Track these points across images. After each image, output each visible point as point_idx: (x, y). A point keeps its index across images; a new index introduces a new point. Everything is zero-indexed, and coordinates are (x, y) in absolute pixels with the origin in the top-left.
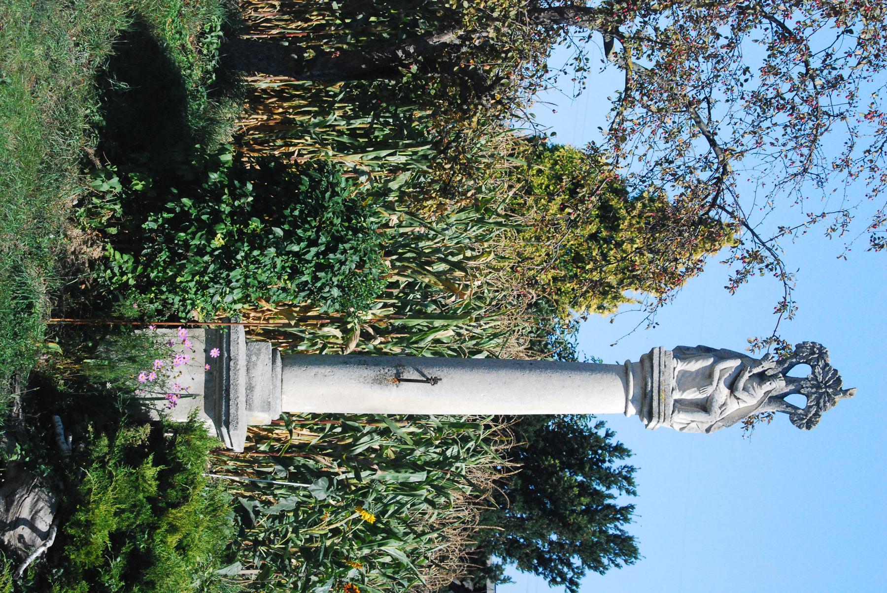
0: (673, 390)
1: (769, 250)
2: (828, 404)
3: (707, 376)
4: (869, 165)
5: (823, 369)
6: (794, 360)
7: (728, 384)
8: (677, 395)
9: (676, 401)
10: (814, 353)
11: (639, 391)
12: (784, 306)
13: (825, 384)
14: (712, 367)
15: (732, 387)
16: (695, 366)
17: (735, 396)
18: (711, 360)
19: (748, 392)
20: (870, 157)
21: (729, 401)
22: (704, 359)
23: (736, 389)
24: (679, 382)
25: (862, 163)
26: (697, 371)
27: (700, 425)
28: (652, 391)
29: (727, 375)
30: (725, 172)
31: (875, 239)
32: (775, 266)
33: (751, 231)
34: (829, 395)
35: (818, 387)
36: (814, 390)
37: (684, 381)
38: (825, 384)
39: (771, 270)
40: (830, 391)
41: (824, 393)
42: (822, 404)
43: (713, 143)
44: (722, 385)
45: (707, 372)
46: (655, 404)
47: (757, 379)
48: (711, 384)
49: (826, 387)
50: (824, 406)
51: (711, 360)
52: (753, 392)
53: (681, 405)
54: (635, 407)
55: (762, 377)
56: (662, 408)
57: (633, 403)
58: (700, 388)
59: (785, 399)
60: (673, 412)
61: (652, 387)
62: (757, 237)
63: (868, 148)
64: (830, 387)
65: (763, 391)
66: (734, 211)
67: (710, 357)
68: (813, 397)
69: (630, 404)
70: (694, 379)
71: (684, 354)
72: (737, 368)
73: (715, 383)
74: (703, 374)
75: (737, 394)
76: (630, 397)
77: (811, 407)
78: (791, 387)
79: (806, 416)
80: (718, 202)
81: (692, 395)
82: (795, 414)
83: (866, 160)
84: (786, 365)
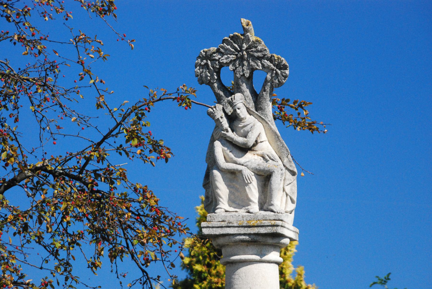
0: (249, 212)
1: (124, 118)
2: (259, 48)
3: (232, 176)
4: (22, 17)
5: (222, 54)
6: (216, 85)
7: (240, 154)
8: (255, 207)
9: (261, 209)
10: (207, 64)
11: (251, 248)
12: (181, 100)
13: (239, 52)
14: (223, 171)
15: (244, 149)
16: (223, 189)
17: (254, 145)
18: (216, 172)
19: (248, 132)
20: (14, 17)
21: (259, 152)
22: (215, 180)
23: (245, 144)
24: (240, 206)
25: (21, 24)
26: (228, 186)
27: (288, 182)
28: (249, 235)
29: (231, 155)
30: (43, 168)
31: (104, 10)
32: (139, 111)
33: (105, 138)
34: (249, 48)
35: (242, 59)
36: (245, 63)
37: (239, 200)
38: (239, 52)
39: (143, 114)
40: (245, 46)
41: (248, 53)
42: (260, 54)
43: (12, 183)
44: (242, 160)
45: (229, 176)
46: (263, 231)
47: (235, 123)
48: (241, 172)
49: (241, 50)
50: (261, 51)
51: (216, 172)
52: (249, 127)
53: (265, 204)
54: (269, 252)
55: (233, 119)
56: (266, 223)
57: (265, 255)
58: (245, 184)
59: (258, 93)
60: (272, 211)
61: (244, 234)
62: (112, 131)
63: (5, 19)
64: (241, 47)
65: (248, 116)
66: (85, 157)
67: (213, 173)
68: (252, 63)
69: (266, 258)
70: (237, 190)
71: (212, 202)
72: (223, 144)
73: (240, 167)
74: (231, 181)
75: (251, 144)
76: (257, 258)
77: (263, 65)
78: (244, 87)
79: (273, 70)
80: (75, 174)
81: (253, 191)
82: (272, 82)
83: (17, 20)
84: (222, 93)
